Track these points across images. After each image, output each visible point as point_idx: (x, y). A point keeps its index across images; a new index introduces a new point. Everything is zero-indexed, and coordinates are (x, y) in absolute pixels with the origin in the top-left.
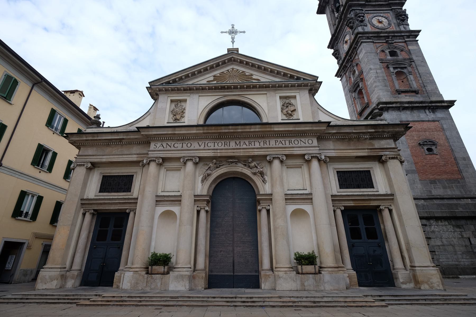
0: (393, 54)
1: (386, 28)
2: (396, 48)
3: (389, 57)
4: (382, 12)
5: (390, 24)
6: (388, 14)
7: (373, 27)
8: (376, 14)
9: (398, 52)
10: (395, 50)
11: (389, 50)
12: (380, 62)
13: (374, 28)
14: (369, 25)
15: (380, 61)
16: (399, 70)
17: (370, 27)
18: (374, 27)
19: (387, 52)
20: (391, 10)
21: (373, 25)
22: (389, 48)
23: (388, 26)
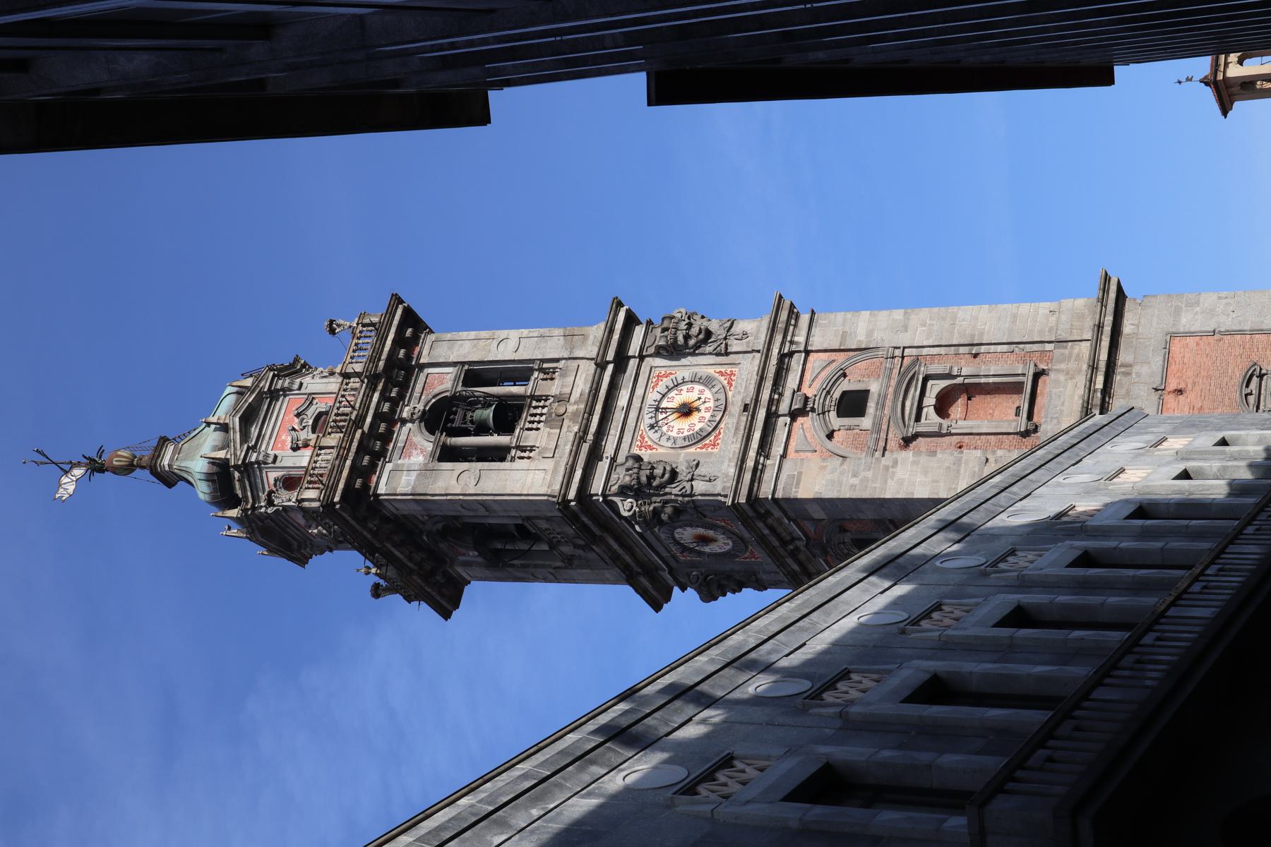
0: (853, 404)
1: (722, 397)
2: (828, 392)
3: (866, 422)
4: (639, 391)
5: (707, 382)
6: (656, 372)
7: (707, 441)
8: (646, 417)
9: (845, 385)
10: (837, 395)
11: (833, 414)
12: (883, 455)
13: (712, 438)
14: (692, 450)
15: (878, 454)
16: (930, 400)
17: (701, 448)
18: (709, 434)
19: (835, 421)
20: (642, 358)
21: (699, 438)
22: (824, 413)
23: (715, 390)
